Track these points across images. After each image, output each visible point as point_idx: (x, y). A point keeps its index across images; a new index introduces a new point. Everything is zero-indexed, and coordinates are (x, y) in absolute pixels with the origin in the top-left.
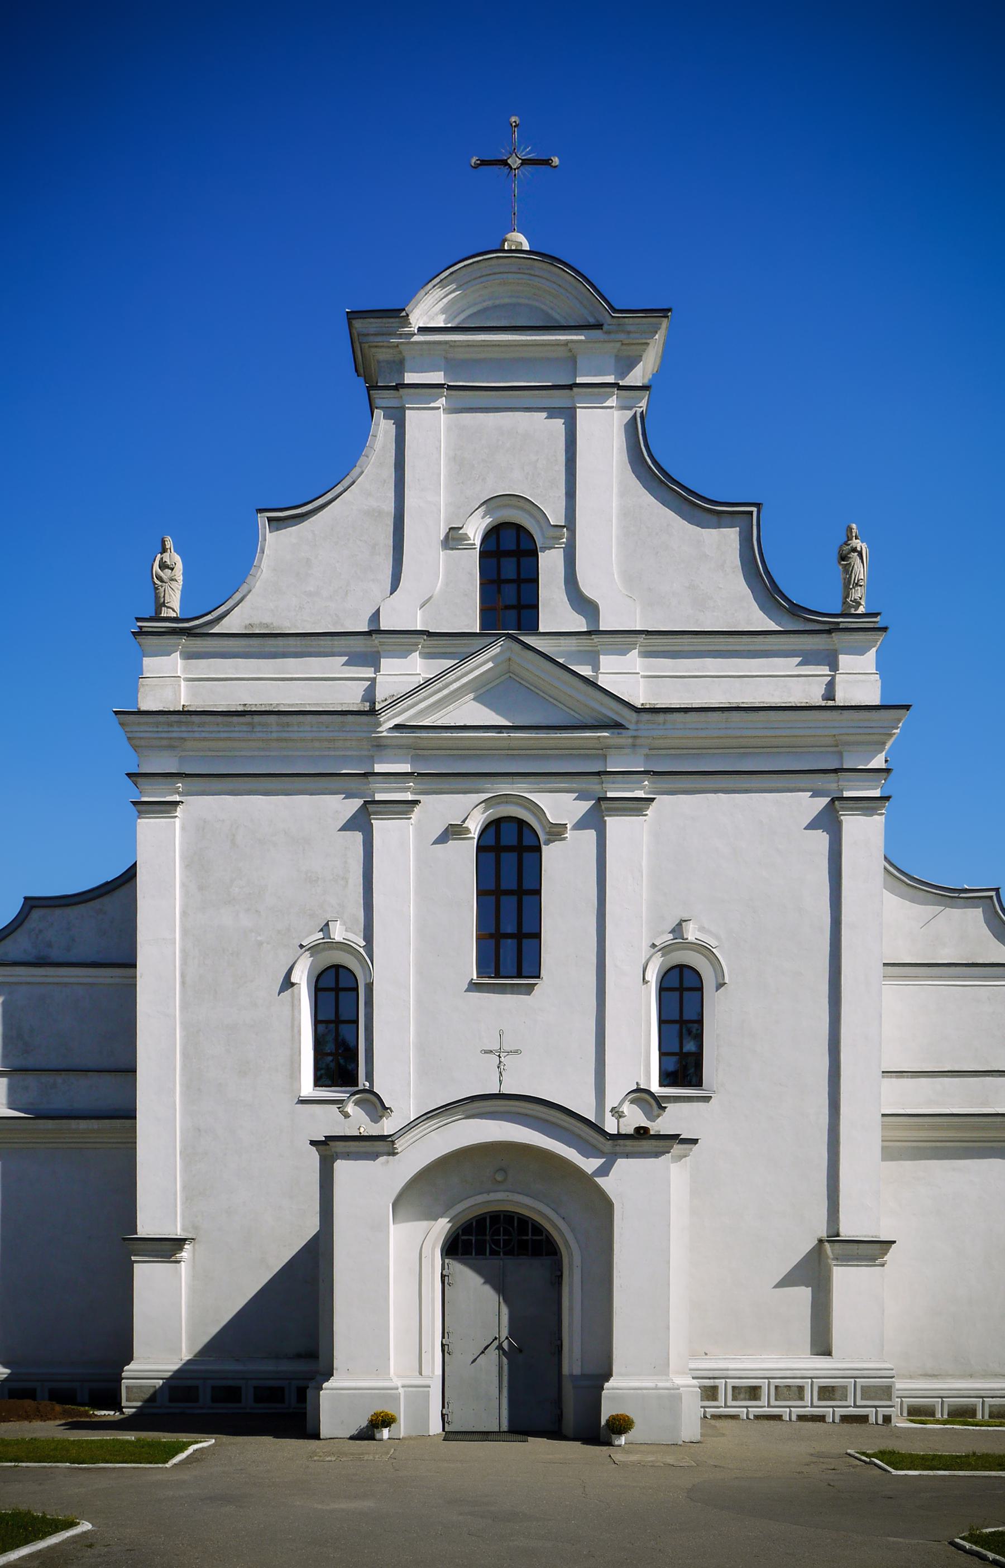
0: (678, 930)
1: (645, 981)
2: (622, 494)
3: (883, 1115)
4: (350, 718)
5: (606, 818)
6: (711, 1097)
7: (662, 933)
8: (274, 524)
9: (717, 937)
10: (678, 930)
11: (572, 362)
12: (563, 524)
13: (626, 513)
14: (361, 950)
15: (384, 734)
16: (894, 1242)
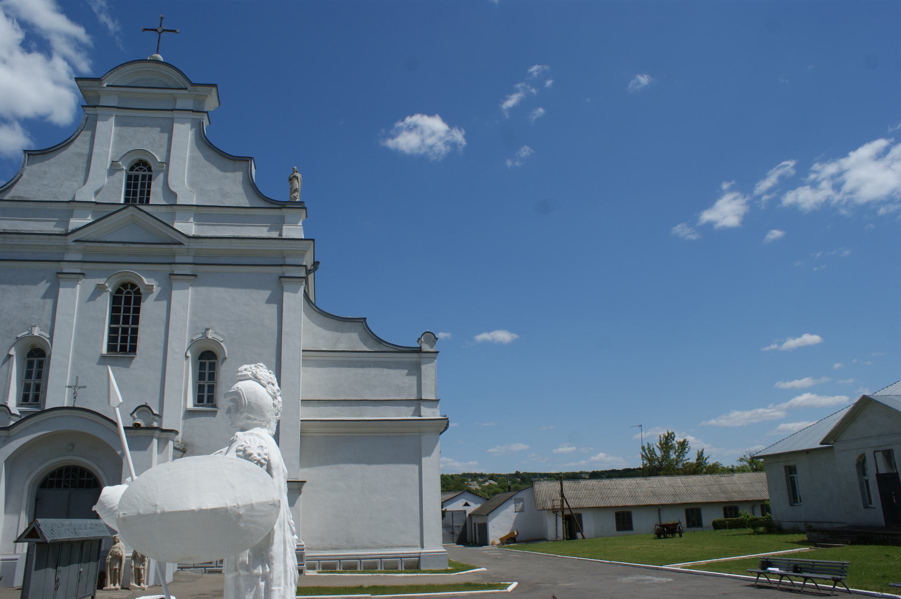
0: (205, 334)
1: (187, 357)
2: (192, 152)
3: (301, 421)
4: (53, 237)
5: (173, 283)
6: (217, 411)
7: (196, 334)
8: (31, 156)
9: (223, 337)
10: (205, 334)
11: (175, 99)
12: (164, 162)
13: (192, 158)
14: (48, 340)
15: (71, 244)
16: (305, 482)
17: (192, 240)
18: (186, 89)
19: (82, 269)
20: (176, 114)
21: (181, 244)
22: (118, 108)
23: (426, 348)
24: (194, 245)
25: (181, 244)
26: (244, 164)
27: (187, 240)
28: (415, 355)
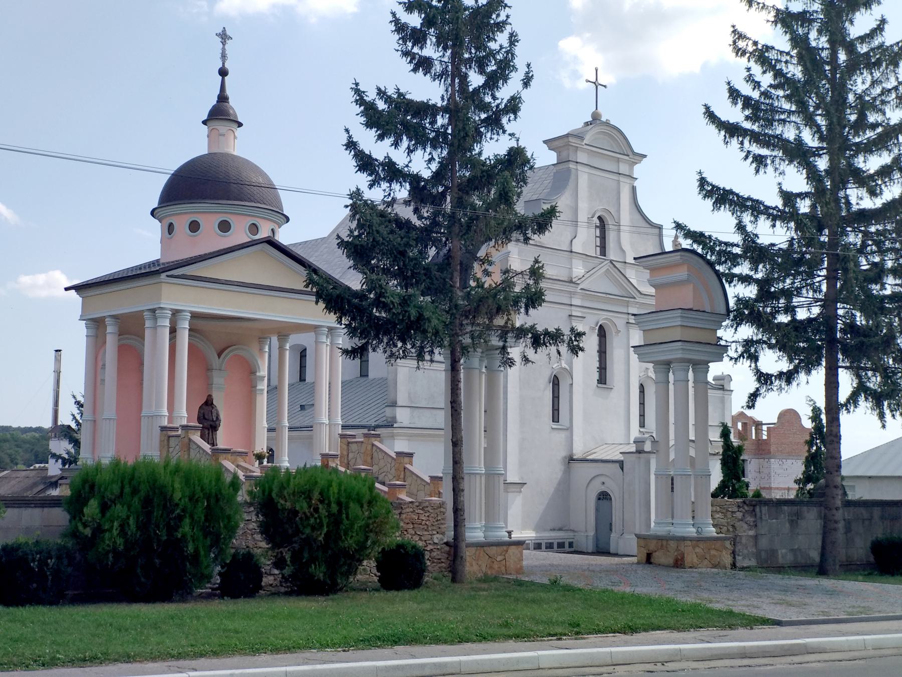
17: (642, 296)
18: (628, 155)
19: (581, 312)
20: (622, 179)
21: (635, 298)
22: (591, 166)
23: (726, 387)
24: (640, 300)
25: (635, 298)
26: (656, 231)
27: (639, 295)
28: (721, 392)
